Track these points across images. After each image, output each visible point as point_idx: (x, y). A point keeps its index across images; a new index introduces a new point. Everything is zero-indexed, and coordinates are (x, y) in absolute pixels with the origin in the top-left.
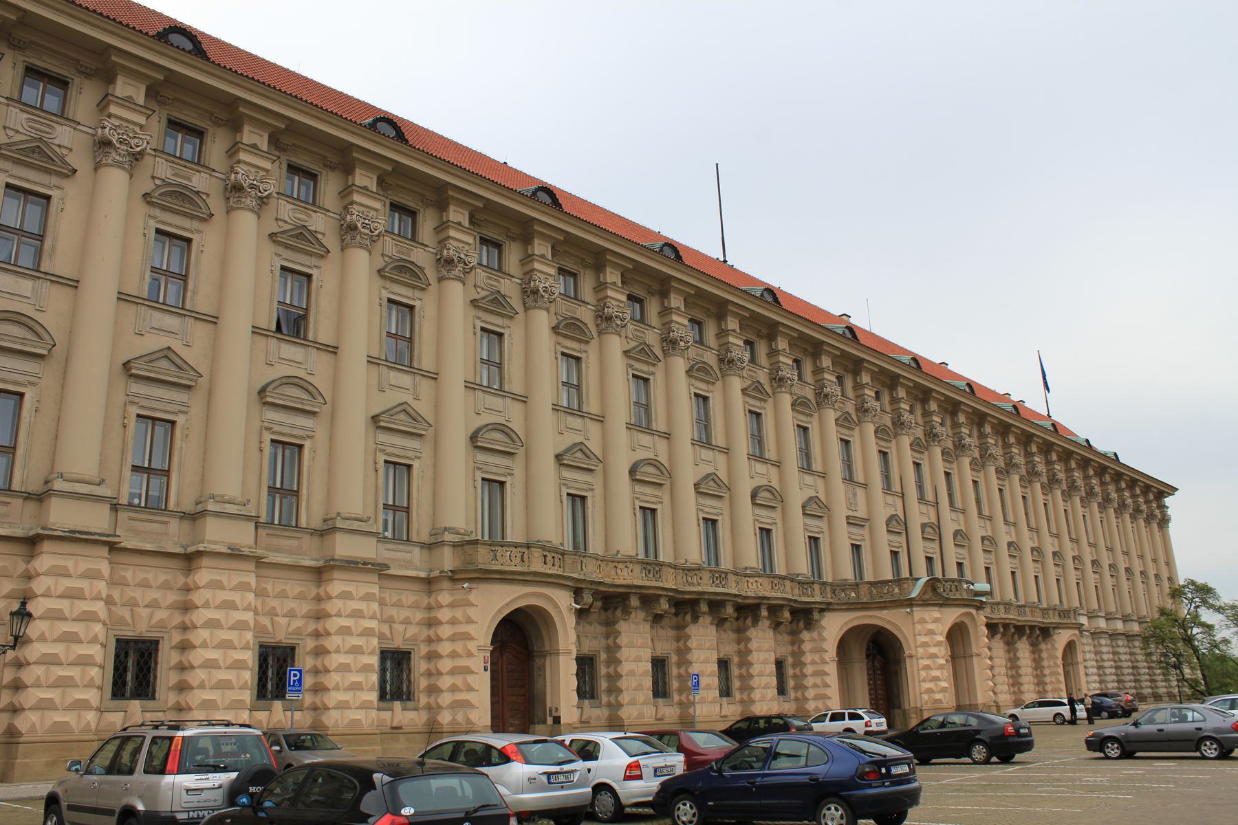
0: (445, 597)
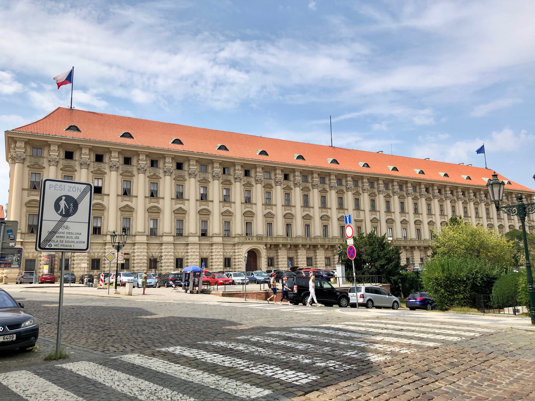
0: (236, 247)
